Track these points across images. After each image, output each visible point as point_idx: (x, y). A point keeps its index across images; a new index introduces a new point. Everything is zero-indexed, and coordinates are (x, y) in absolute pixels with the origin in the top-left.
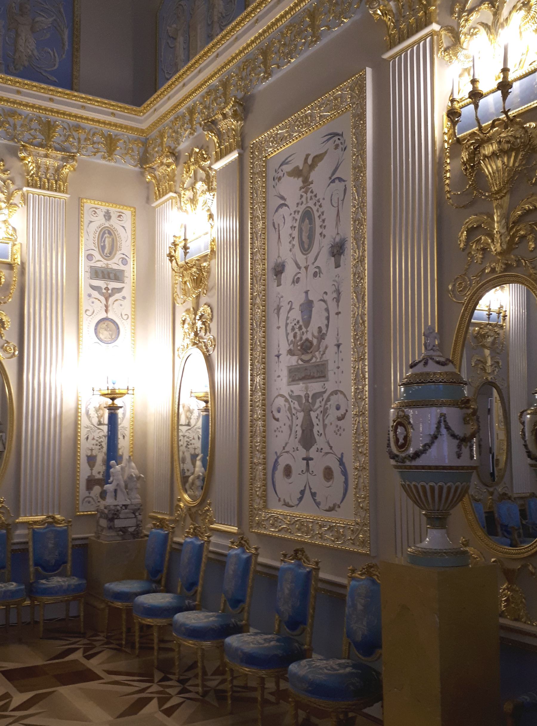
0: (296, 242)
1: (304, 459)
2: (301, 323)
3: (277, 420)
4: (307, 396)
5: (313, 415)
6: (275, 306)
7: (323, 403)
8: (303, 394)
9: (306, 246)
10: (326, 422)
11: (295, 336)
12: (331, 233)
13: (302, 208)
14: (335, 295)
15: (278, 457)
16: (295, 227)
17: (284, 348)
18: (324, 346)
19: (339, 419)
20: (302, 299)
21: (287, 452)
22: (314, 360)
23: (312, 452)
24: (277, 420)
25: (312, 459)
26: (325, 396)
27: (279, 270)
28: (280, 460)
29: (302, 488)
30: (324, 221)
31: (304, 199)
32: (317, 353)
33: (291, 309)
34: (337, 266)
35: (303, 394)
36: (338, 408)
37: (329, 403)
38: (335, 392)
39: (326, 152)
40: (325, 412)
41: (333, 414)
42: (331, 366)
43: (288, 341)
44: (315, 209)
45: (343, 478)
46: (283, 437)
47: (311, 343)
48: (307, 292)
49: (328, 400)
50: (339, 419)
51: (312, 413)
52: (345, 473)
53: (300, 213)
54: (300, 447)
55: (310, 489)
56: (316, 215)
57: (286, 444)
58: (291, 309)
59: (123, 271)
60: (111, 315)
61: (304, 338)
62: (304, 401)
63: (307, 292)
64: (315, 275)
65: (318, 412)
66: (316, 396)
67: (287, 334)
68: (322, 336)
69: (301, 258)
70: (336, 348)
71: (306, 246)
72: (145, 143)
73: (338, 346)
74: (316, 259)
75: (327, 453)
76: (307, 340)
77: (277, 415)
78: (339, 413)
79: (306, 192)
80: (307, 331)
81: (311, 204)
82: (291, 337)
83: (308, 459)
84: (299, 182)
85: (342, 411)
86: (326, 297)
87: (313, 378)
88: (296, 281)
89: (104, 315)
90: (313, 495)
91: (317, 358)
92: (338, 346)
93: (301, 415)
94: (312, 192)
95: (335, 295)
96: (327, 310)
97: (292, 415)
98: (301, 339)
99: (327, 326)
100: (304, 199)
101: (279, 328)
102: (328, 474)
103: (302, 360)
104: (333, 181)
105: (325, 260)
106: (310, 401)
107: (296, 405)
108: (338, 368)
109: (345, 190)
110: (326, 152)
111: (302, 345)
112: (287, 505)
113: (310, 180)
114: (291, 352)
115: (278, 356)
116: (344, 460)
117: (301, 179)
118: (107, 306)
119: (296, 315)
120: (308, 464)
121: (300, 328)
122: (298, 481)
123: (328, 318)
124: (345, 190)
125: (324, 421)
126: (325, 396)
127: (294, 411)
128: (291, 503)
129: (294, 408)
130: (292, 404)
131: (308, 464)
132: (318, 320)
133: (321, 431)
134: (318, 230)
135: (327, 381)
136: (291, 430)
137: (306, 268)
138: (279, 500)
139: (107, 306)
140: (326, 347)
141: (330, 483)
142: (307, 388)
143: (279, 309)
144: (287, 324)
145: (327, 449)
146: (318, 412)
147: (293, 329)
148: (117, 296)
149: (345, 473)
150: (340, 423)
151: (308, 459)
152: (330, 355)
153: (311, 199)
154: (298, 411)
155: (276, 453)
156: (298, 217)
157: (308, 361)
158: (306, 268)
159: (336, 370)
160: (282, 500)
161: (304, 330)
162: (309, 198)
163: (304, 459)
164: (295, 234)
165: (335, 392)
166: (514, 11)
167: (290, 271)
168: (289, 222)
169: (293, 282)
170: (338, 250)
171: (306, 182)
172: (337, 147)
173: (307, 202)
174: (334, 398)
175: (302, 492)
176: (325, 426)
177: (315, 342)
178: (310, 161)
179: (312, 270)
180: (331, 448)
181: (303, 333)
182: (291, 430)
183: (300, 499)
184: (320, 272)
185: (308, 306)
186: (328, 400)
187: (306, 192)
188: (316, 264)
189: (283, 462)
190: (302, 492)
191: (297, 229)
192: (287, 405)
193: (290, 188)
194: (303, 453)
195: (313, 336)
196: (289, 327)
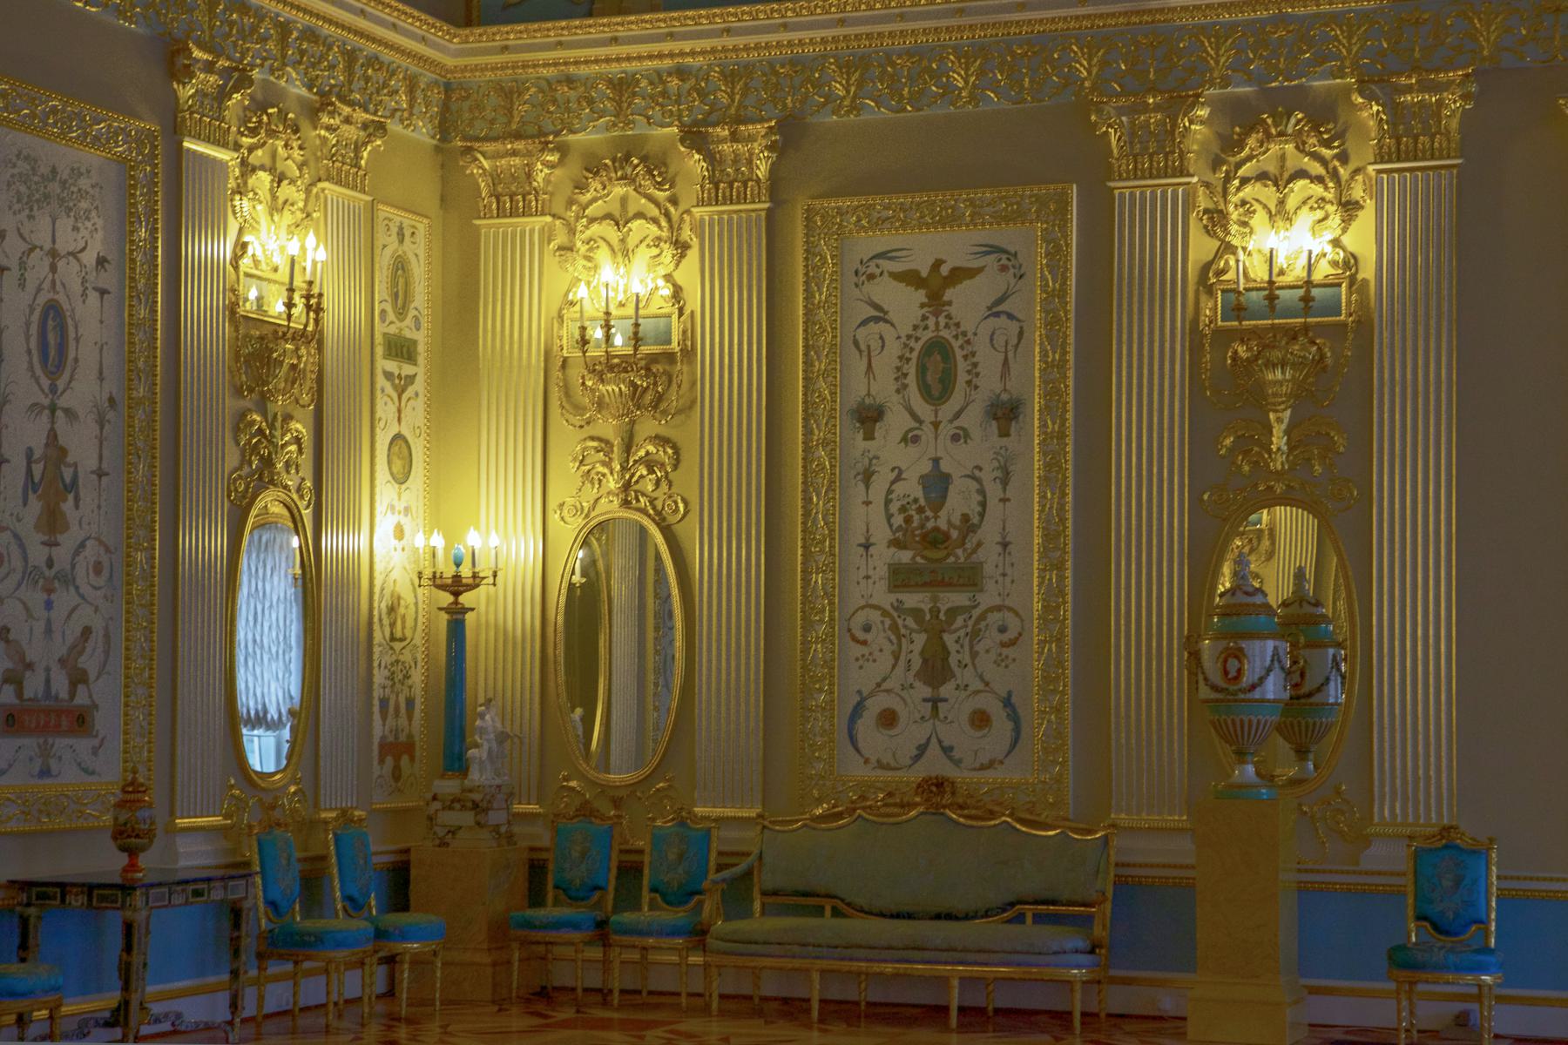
0: (911, 380)
1: (925, 700)
2: (922, 502)
3: (864, 643)
4: (935, 612)
5: (949, 639)
6: (860, 467)
7: (970, 623)
8: (926, 607)
9: (936, 393)
10: (977, 648)
11: (908, 520)
12: (990, 383)
13: (927, 335)
14: (998, 474)
15: (863, 700)
16: (908, 360)
17: (881, 534)
18: (975, 541)
19: (1003, 645)
20: (926, 467)
21: (887, 691)
22: (952, 559)
23: (946, 690)
24: (864, 643)
25: (946, 700)
26: (976, 613)
27: (869, 417)
28: (868, 703)
29: (923, 742)
30: (975, 365)
31: (931, 322)
32: (959, 552)
33: (898, 479)
34: (1004, 433)
35: (926, 607)
36: (1003, 630)
37: (983, 625)
38: (999, 608)
39: (980, 270)
40: (975, 635)
41: (991, 639)
42: (988, 569)
43: (891, 526)
44: (956, 344)
45: (1010, 725)
46: (878, 668)
47: (947, 536)
48: (936, 461)
49: (982, 617)
50: (1003, 645)
51: (946, 636)
52: (1015, 718)
53: (921, 343)
54: (918, 684)
55: (940, 742)
56: (959, 354)
57: (884, 680)
58: (898, 479)
59: (415, 342)
60: (405, 432)
61: (930, 525)
62: (928, 617)
63: (936, 461)
64: (955, 438)
65: (962, 633)
66: (953, 612)
67: (889, 517)
68: (968, 526)
69: (924, 410)
70: (999, 549)
71: (936, 393)
72: (448, 88)
73: (1005, 545)
74: (957, 415)
75: (977, 692)
76: (936, 529)
77: (860, 635)
78: (1005, 637)
79: (936, 315)
80: (936, 517)
81: (945, 333)
82: (898, 520)
83: (935, 702)
84: (921, 296)
85: (1011, 634)
86: (977, 473)
87: (950, 585)
88: (910, 439)
89: (394, 430)
90: (947, 750)
91: (957, 557)
92: (1005, 545)
93: (920, 639)
94: (949, 317)
95: (998, 474)
96: (982, 492)
97: (899, 637)
98: (922, 526)
99: (982, 515)
100: (931, 322)
101: (867, 503)
102: (981, 720)
103: (923, 557)
104: (997, 315)
105: (973, 419)
106: (942, 616)
107: (910, 622)
108: (1004, 575)
109: (1021, 334)
110: (980, 270)
111: (924, 536)
112: (887, 767)
113: (945, 298)
114: (896, 543)
115: (867, 547)
116: (1014, 699)
117: (922, 292)
118: (399, 411)
119: (911, 488)
120: (935, 708)
121: (920, 510)
122: (910, 733)
123: (983, 504)
124: (1021, 334)
125: (971, 647)
126: (976, 613)
127: (903, 631)
128: (893, 764)
129: (905, 627)
130: (900, 622)
131: (935, 708)
132: (959, 502)
133: (967, 659)
134: (962, 377)
135: (981, 590)
136: (897, 659)
137: (936, 425)
138: (867, 761)
139: (399, 411)
140: (979, 544)
141: (980, 734)
142: (935, 599)
143: (867, 476)
144: (888, 502)
145: (976, 685)
146: (962, 633)
147: (903, 509)
148: (410, 392)
149: (1015, 718)
150: (1005, 651)
151: (935, 702)
152: (989, 556)
153: (947, 326)
154: (912, 631)
155: (859, 692)
156: (918, 346)
157: (937, 560)
158: (936, 425)
159: (1000, 579)
160: (873, 759)
161: (929, 513)
162: (942, 324)
163: (925, 700)
164: (911, 369)
165: (999, 608)
166: (1305, 209)
167: (896, 421)
168: (893, 348)
169: (904, 439)
170: (1006, 413)
171: (936, 301)
172: (1004, 268)
173: (937, 329)
174: (994, 618)
175: (922, 749)
176: (974, 655)
177: (955, 534)
178: (945, 270)
179: (947, 430)
180: (987, 684)
181: (927, 519)
182: (897, 659)
183: (917, 758)
184: (967, 436)
185: (937, 483)
186: (982, 617)
187: (936, 315)
188: (956, 423)
189: (875, 706)
190: (922, 749)
191: (914, 361)
192: (888, 622)
193: (905, 304)
194: (927, 692)
195: (949, 522)
196: (894, 507)
